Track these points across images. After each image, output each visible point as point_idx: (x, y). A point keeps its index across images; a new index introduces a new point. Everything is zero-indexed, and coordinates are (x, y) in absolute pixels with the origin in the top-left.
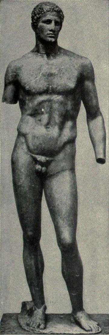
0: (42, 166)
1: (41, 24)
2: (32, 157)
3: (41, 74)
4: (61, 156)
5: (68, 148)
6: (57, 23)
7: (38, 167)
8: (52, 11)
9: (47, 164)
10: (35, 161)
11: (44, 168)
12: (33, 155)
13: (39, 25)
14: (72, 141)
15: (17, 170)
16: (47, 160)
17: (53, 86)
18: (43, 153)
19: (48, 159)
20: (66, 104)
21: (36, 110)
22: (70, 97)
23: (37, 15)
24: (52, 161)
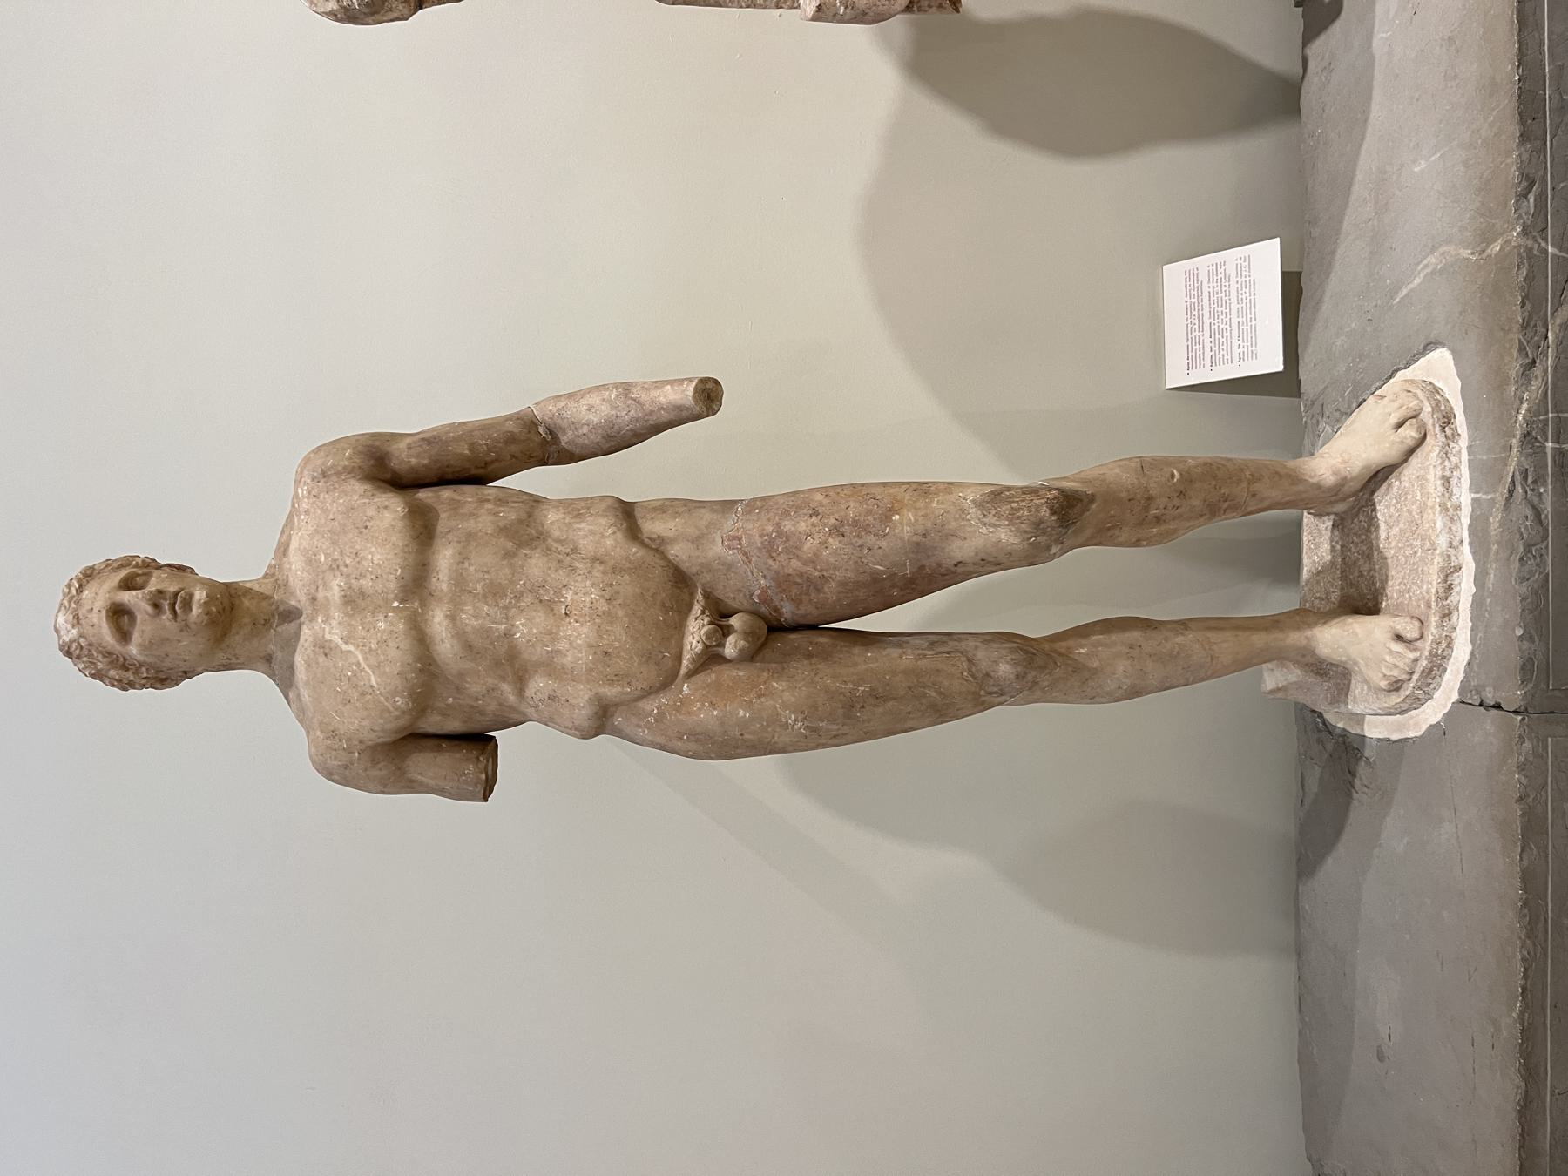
0: (726, 631)
1: (133, 650)
2: (691, 674)
3: (344, 647)
4: (678, 552)
5: (653, 527)
6: (128, 584)
7: (731, 647)
8: (77, 603)
9: (720, 615)
10: (710, 657)
11: (735, 621)
12: (683, 670)
13: (140, 658)
14: (627, 513)
15: (747, 736)
16: (703, 613)
17: (391, 596)
18: (680, 628)
19: (697, 609)
20: (470, 536)
21: (497, 663)
22: (444, 522)
23: (100, 666)
24: (707, 596)
